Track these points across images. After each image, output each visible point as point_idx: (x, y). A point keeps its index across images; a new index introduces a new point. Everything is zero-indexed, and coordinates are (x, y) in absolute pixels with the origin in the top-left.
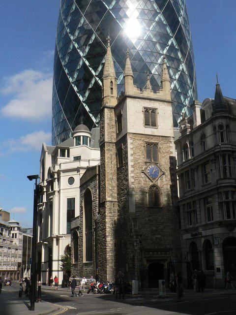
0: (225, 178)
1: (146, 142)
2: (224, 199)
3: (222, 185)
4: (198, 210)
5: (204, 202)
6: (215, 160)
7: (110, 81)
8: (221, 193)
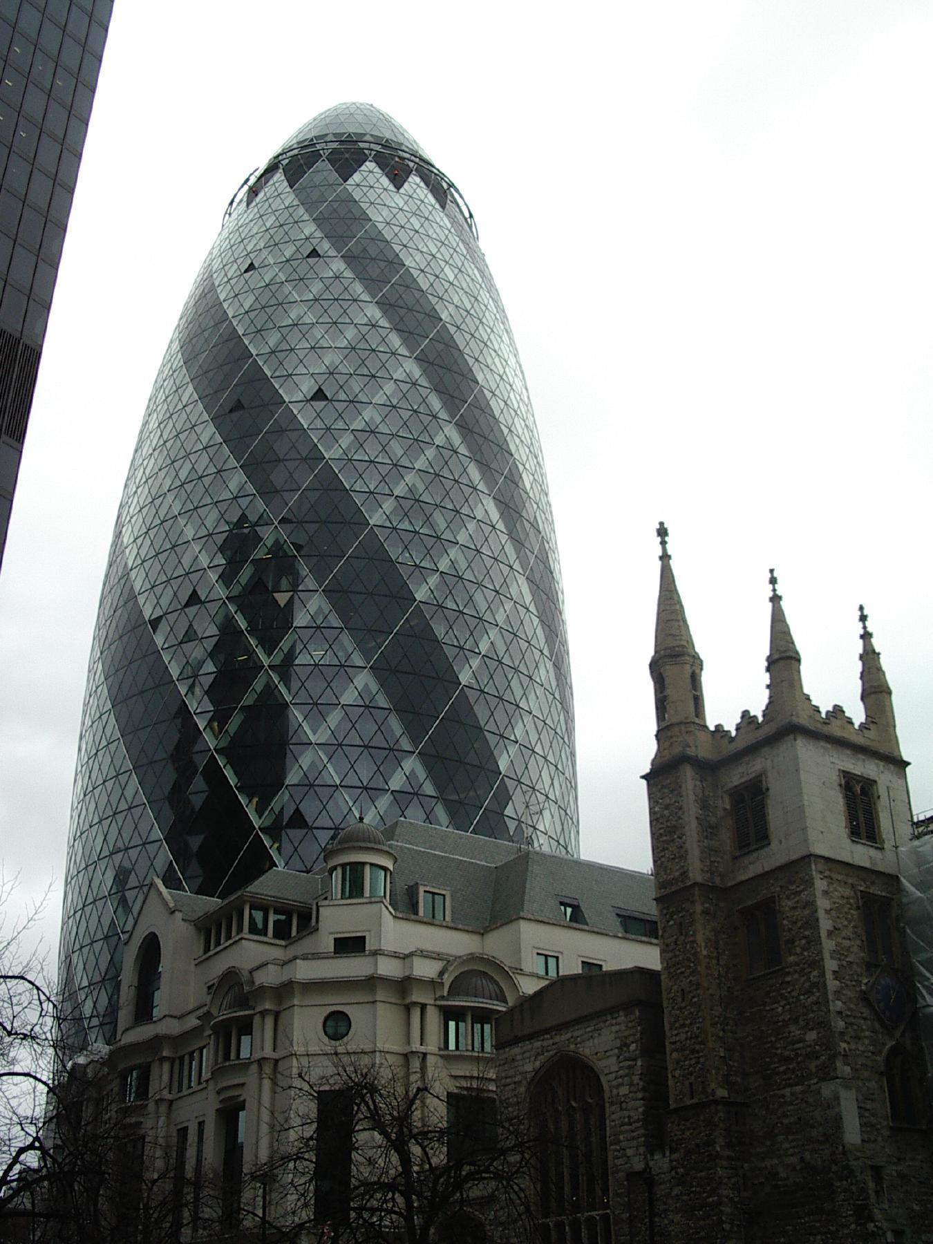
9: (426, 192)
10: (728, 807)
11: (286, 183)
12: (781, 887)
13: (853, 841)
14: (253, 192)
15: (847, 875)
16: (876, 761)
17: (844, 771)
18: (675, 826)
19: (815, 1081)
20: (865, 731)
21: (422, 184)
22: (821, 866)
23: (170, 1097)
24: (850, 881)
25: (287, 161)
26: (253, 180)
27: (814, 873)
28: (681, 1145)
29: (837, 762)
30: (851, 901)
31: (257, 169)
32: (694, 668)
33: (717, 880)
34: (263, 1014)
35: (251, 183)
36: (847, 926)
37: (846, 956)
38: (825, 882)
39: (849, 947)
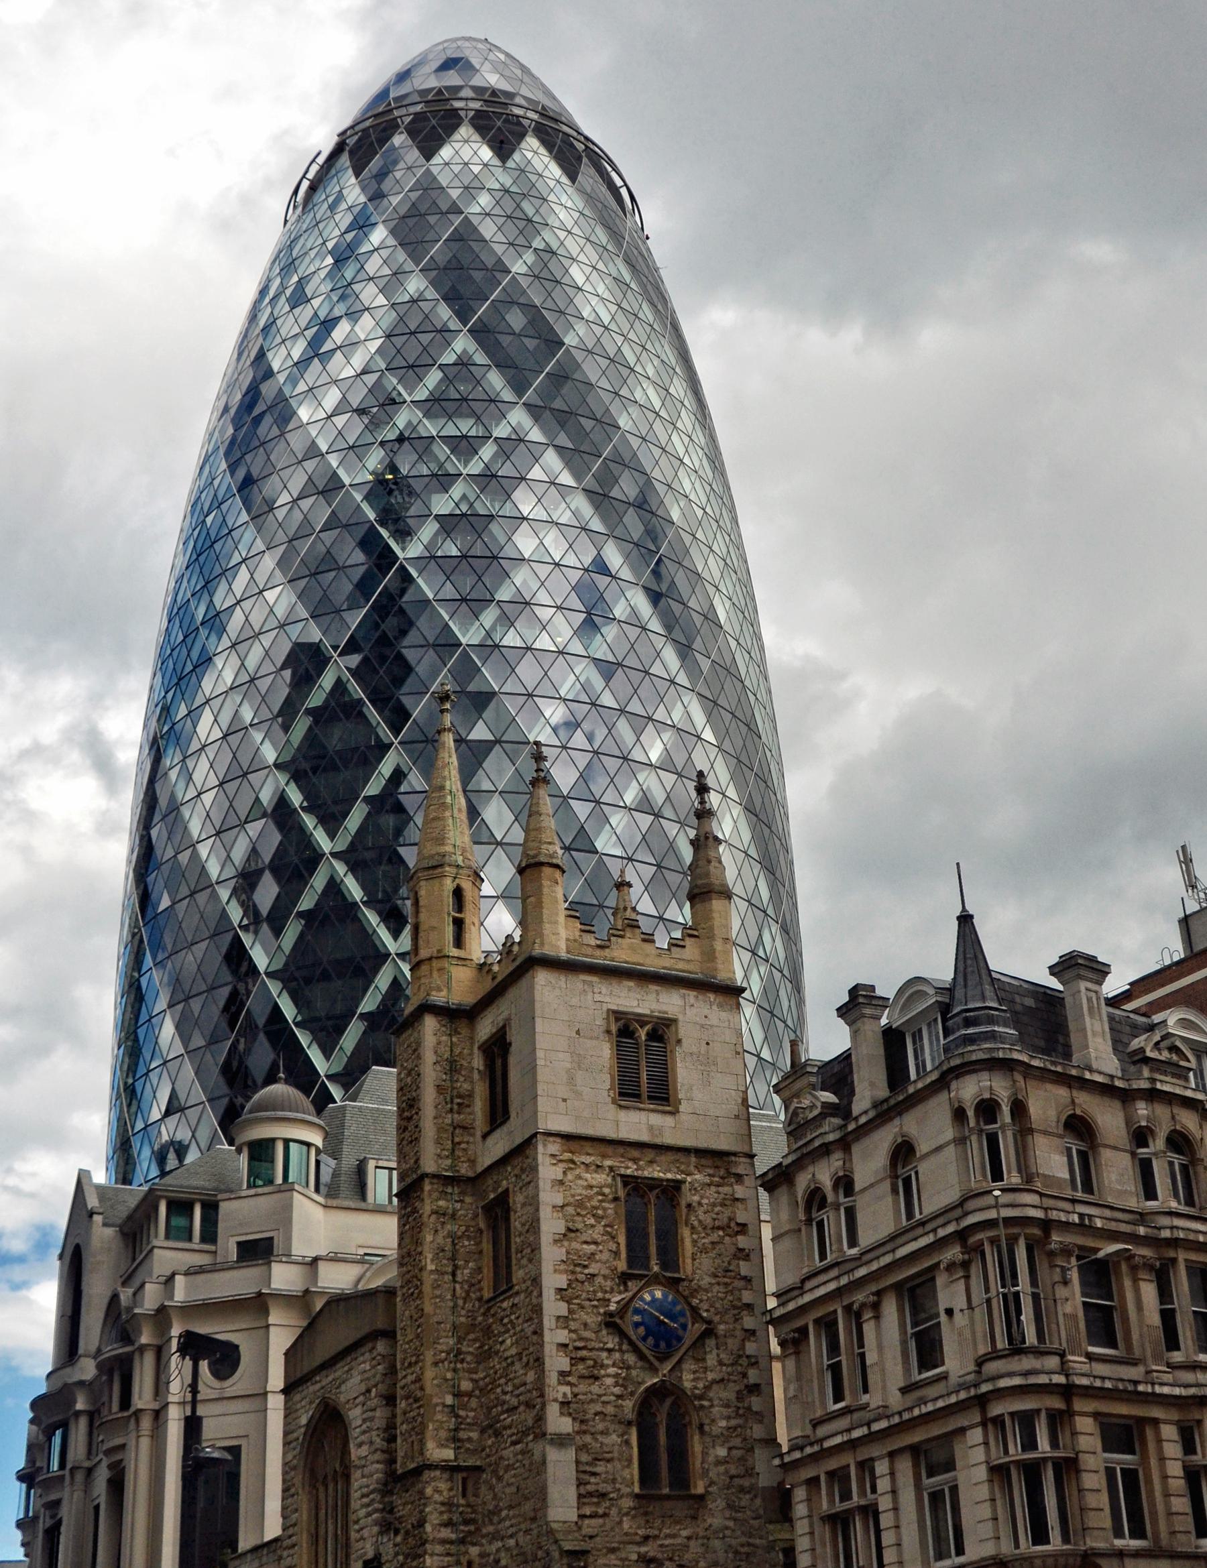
0: (1017, 1349)
1: (627, 1180)
2: (1015, 1451)
3: (1004, 1383)
4: (885, 1503)
5: (916, 1466)
6: (965, 1265)
7: (449, 885)
8: (998, 1421)
9: (546, 160)
10: (481, 1068)
11: (350, 171)
12: (516, 1176)
13: (621, 1107)
14: (313, 188)
15: (604, 1156)
16: (683, 991)
17: (615, 1012)
18: (414, 1099)
19: (531, 1437)
20: (674, 949)
21: (542, 150)
22: (554, 1147)
23: (87, 1464)
24: (608, 1163)
25: (356, 137)
26: (315, 168)
27: (540, 1158)
28: (401, 1523)
29: (607, 999)
30: (607, 1191)
31: (319, 154)
32: (457, 881)
33: (464, 1170)
34: (142, 1349)
35: (310, 175)
36: (593, 1226)
37: (585, 1267)
38: (559, 1170)
39: (593, 1254)
